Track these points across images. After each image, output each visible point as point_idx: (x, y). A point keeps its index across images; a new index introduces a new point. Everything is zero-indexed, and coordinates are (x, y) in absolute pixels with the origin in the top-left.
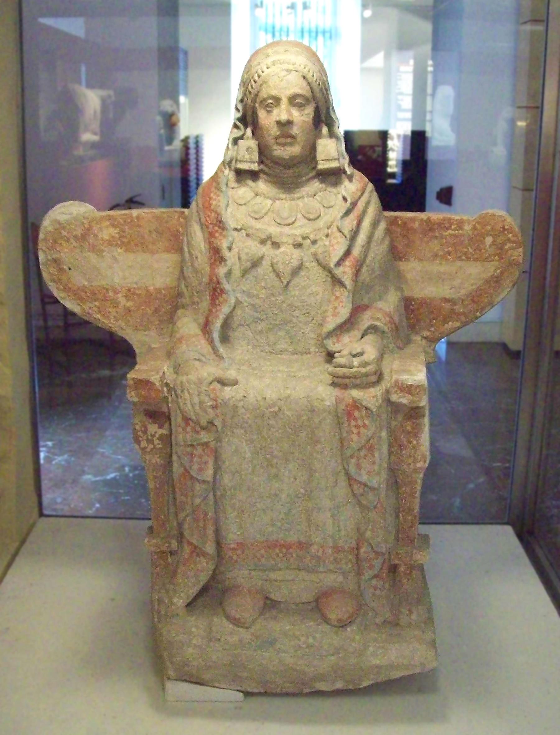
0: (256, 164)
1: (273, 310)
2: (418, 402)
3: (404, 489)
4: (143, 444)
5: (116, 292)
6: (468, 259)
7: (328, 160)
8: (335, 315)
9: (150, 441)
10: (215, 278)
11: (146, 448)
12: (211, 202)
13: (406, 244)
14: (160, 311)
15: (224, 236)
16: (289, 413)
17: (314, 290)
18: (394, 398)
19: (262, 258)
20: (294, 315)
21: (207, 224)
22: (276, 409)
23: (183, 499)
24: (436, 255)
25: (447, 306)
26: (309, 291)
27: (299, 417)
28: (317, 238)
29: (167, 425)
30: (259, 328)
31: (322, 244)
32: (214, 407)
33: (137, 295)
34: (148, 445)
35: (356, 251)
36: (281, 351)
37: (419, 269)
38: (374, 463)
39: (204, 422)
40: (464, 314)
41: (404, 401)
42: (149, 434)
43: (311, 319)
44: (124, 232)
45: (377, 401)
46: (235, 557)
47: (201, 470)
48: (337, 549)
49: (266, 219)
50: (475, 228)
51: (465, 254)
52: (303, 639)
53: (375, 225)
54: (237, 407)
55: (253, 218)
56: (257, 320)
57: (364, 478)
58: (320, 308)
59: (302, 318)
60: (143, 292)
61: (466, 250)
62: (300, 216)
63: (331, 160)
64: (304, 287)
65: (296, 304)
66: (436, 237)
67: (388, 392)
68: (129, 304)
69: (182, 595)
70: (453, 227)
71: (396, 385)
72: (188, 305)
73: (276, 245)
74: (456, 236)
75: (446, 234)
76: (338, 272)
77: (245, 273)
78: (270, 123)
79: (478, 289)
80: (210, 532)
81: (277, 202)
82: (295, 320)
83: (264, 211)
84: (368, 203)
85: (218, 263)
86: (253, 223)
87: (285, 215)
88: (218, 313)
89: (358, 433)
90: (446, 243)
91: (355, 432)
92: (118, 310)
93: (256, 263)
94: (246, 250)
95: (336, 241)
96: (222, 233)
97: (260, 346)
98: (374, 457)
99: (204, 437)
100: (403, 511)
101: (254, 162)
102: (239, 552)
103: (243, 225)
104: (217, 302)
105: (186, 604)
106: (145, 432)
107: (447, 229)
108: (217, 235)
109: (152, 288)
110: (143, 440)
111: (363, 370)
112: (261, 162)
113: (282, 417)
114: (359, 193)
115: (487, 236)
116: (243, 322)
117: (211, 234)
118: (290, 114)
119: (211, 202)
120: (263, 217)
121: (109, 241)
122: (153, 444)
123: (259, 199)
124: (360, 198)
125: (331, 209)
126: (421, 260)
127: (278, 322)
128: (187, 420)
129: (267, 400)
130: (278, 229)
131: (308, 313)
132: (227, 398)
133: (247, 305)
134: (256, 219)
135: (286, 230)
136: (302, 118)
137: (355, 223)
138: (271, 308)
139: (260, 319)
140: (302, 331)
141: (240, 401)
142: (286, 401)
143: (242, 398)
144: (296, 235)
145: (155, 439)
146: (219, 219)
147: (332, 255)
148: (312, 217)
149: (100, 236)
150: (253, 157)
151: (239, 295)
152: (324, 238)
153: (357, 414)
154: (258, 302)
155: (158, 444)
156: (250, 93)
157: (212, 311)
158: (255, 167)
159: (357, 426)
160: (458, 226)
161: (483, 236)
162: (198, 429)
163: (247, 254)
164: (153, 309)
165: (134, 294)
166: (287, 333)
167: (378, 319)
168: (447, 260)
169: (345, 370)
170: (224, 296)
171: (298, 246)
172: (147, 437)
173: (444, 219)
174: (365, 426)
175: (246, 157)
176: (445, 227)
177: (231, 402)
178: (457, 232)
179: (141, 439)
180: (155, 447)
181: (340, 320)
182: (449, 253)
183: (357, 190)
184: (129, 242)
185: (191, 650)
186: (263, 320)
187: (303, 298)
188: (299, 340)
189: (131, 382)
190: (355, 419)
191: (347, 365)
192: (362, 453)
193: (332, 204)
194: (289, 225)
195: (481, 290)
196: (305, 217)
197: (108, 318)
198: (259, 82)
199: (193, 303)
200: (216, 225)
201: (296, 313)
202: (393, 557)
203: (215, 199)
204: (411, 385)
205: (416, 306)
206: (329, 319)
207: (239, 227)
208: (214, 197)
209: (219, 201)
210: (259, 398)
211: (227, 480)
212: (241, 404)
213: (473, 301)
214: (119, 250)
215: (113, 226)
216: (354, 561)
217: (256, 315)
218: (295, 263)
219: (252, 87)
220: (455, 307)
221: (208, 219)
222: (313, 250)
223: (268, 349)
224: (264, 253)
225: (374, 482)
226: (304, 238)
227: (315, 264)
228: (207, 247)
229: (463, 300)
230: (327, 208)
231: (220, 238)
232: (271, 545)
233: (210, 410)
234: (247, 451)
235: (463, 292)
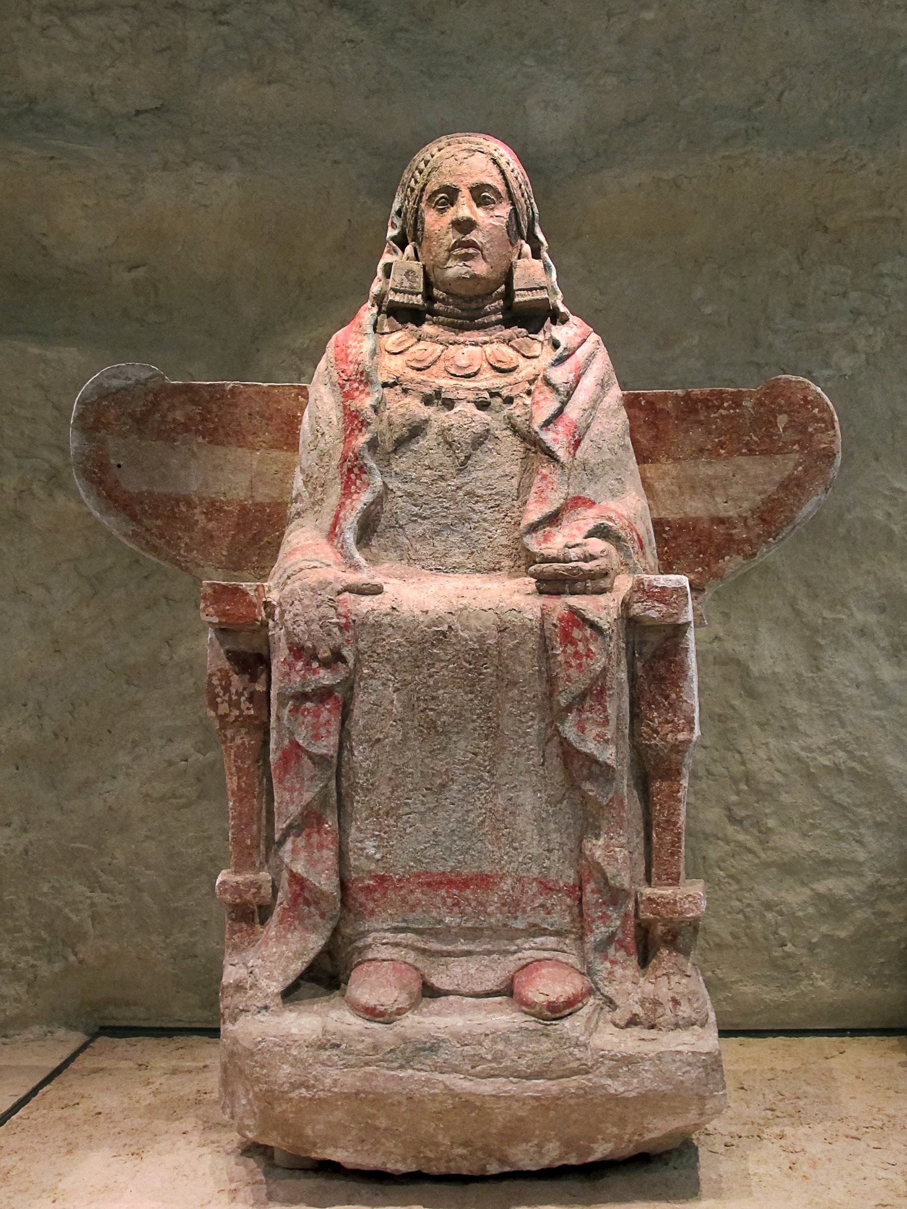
0: (420, 296)
1: (442, 502)
2: (676, 617)
3: (658, 784)
4: (223, 709)
5: (190, 504)
6: (751, 452)
7: (531, 290)
8: (542, 500)
9: (235, 705)
10: (351, 454)
11: (226, 715)
13: (653, 437)
14: (261, 540)
15: (368, 394)
16: (465, 635)
17: (508, 471)
18: (637, 609)
19: (426, 421)
20: (476, 508)
21: (341, 382)
22: (445, 628)
23: (287, 796)
24: (701, 450)
25: (721, 530)
26: (499, 472)
27: (482, 639)
28: (513, 394)
29: (264, 676)
30: (420, 530)
31: (521, 403)
32: (343, 628)
33: (225, 511)
34: (231, 711)
35: (573, 412)
36: (454, 568)
37: (674, 473)
38: (606, 721)
39: (324, 653)
40: (748, 541)
41: (653, 614)
42: (233, 690)
43: (502, 515)
44: (209, 412)
45: (608, 614)
46: (371, 905)
47: (317, 737)
48: (546, 887)
49: (434, 369)
50: (760, 403)
51: (747, 444)
52: (487, 1043)
53: (603, 385)
54: (381, 625)
55: (413, 368)
56: (416, 518)
57: (591, 747)
58: (518, 497)
59: (489, 514)
60: (234, 509)
61: (748, 438)
62: (485, 365)
63: (536, 289)
64: (491, 466)
65: (479, 492)
66: (701, 423)
67: (626, 605)
68: (211, 525)
69: (276, 974)
70: (726, 405)
71: (639, 587)
73: (449, 404)
74: (732, 418)
75: (716, 415)
76: (548, 437)
77: (400, 443)
79: (770, 499)
80: (329, 855)
81: (451, 347)
82: (475, 517)
83: (431, 359)
84: (592, 355)
85: (356, 432)
86: (413, 374)
87: (463, 362)
89: (580, 665)
90: (716, 429)
91: (573, 664)
92: (193, 535)
93: (416, 430)
94: (401, 411)
95: (542, 397)
97: (419, 560)
98: (605, 711)
99: (325, 677)
100: (658, 825)
101: (417, 294)
102: (377, 895)
103: (398, 378)
105: (281, 989)
106: (226, 689)
107: (719, 407)
109: (251, 502)
110: (222, 703)
111: (586, 566)
112: (429, 297)
113: (454, 640)
114: (579, 340)
115: (780, 414)
116: (393, 523)
117: (347, 396)
118: (473, 212)
119: (349, 351)
120: (428, 367)
121: (185, 424)
122: (239, 708)
123: (422, 345)
124: (579, 347)
125: (534, 360)
126: (677, 460)
127: (449, 521)
128: (297, 651)
129: (429, 613)
130: (453, 382)
131: (498, 506)
132: (365, 611)
133: (400, 494)
134: (419, 369)
135: (466, 383)
136: (491, 221)
137: (571, 376)
138: (440, 497)
139: (420, 517)
140: (490, 534)
141: (386, 615)
142: (459, 616)
143: (389, 610)
144: (479, 390)
145: (243, 699)
147: (535, 415)
148: (505, 367)
149: (170, 417)
150: (415, 285)
151: (387, 480)
152: (525, 396)
153: (576, 634)
154: (421, 489)
155: (248, 709)
156: (413, 190)
158: (418, 300)
159: (577, 655)
160: (733, 403)
161: (773, 413)
162: (315, 665)
163: (403, 415)
164: (249, 536)
165: (220, 510)
166: (465, 538)
167: (610, 519)
168: (719, 455)
169: (556, 566)
170: (364, 476)
171: (483, 405)
172: (230, 698)
173: (712, 393)
174: (589, 654)
175: (404, 285)
176: (714, 406)
177: (371, 618)
178: (732, 411)
179: (219, 700)
180: (241, 715)
181: (548, 509)
182: (721, 445)
183: (576, 335)
184: (215, 429)
185: (287, 1069)
186: (425, 518)
187: (489, 482)
188: (483, 549)
189: (209, 591)
190: (573, 642)
191: (561, 557)
192: (588, 702)
193: (537, 354)
194: (468, 376)
195: (774, 500)
196: (495, 368)
197: (177, 547)
198: (426, 171)
200: (355, 381)
201: (480, 507)
202: (642, 907)
203: (355, 347)
204: (664, 589)
205: (671, 533)
206: (530, 507)
207: (392, 381)
209: (361, 347)
210: (417, 612)
211: (360, 754)
212: (387, 620)
213: (764, 521)
214: (200, 439)
215: (193, 402)
216: (576, 910)
217: (416, 509)
218: (480, 429)
220: (734, 531)
221: (342, 374)
222: (506, 412)
223: (434, 564)
224: (430, 416)
225: (609, 755)
226: (492, 395)
227: (508, 432)
228: (340, 415)
229: (746, 519)
230: (528, 358)
231: (363, 396)
232: (433, 883)
233: (336, 630)
234: (396, 703)
235: (746, 505)
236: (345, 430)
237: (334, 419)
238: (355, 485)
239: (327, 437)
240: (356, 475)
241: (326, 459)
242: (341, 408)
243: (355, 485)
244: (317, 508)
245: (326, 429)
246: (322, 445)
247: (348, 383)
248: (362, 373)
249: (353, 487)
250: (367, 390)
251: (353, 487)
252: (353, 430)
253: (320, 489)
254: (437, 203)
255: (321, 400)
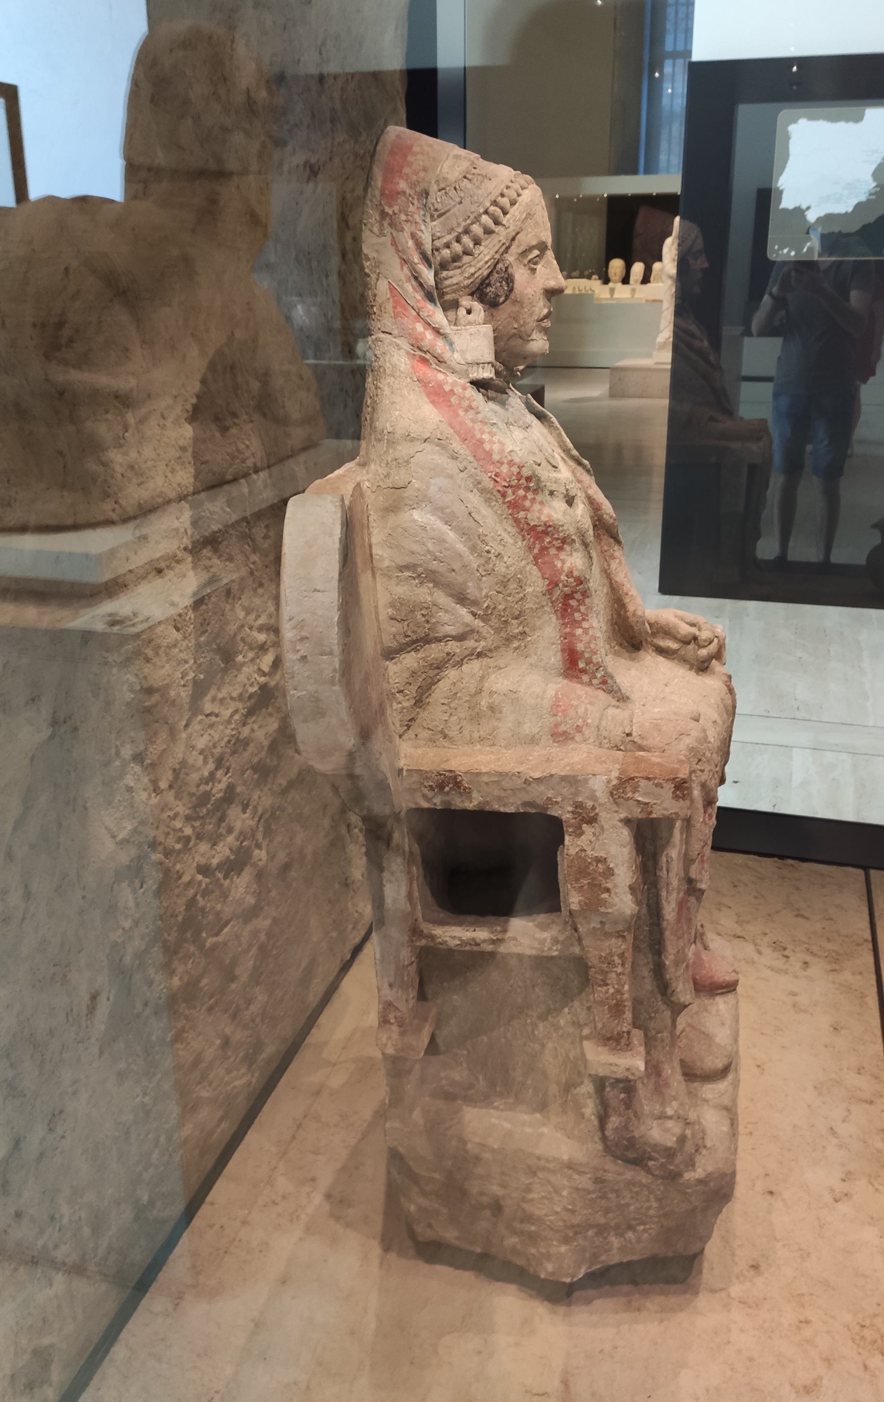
12: (487, 447)
72: (497, 648)
78: (535, 292)
85: (553, 551)
88: (591, 633)
96: (534, 499)
104: (577, 616)
108: (527, 504)
117: (515, 506)
146: (526, 472)
157: (573, 635)
170: (587, 601)
199: (508, 640)
200: (518, 487)
208: (486, 437)
219: (497, 222)
228: (513, 530)
231: (537, 507)
236: (530, 548)
237: (505, 535)
238: (579, 611)
239: (506, 559)
240: (578, 601)
241: (512, 586)
242: (510, 522)
243: (579, 611)
244: (516, 644)
245: (500, 549)
246: (501, 568)
247: (510, 491)
248: (529, 479)
249: (576, 615)
250: (539, 498)
251: (576, 615)
252: (543, 549)
253: (514, 622)
254: (529, 261)
255: (479, 512)
